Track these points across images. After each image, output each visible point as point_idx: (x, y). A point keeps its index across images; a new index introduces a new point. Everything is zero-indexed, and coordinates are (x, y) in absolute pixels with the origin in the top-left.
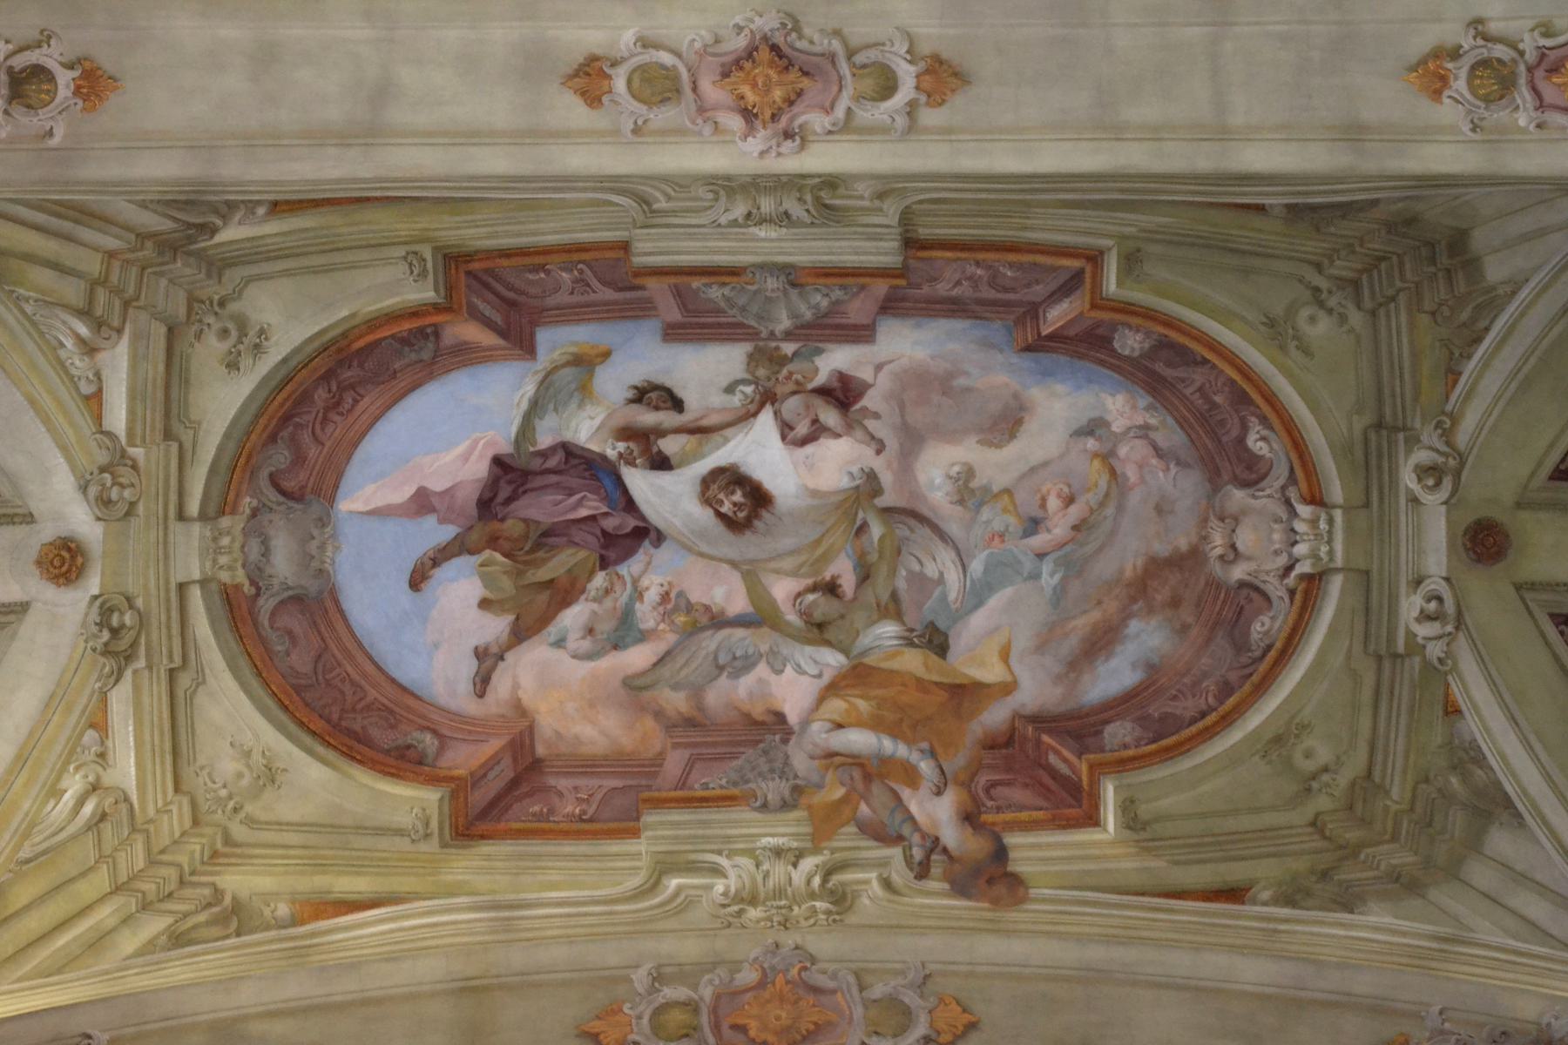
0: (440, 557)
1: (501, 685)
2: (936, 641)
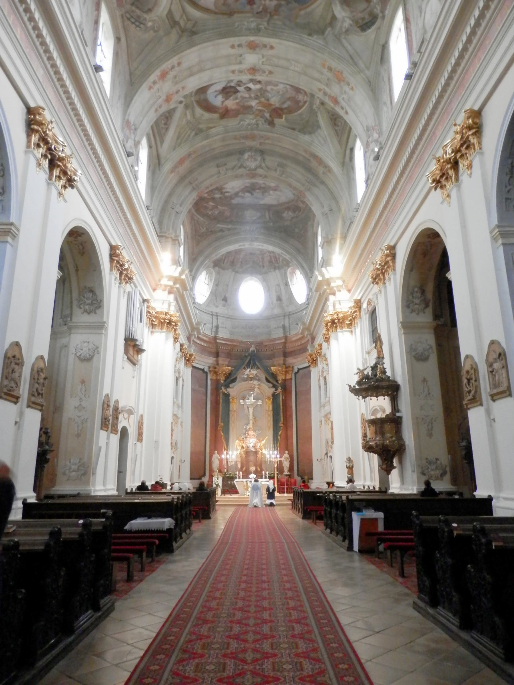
0: (217, 95)
1: (224, 104)
2: (268, 100)
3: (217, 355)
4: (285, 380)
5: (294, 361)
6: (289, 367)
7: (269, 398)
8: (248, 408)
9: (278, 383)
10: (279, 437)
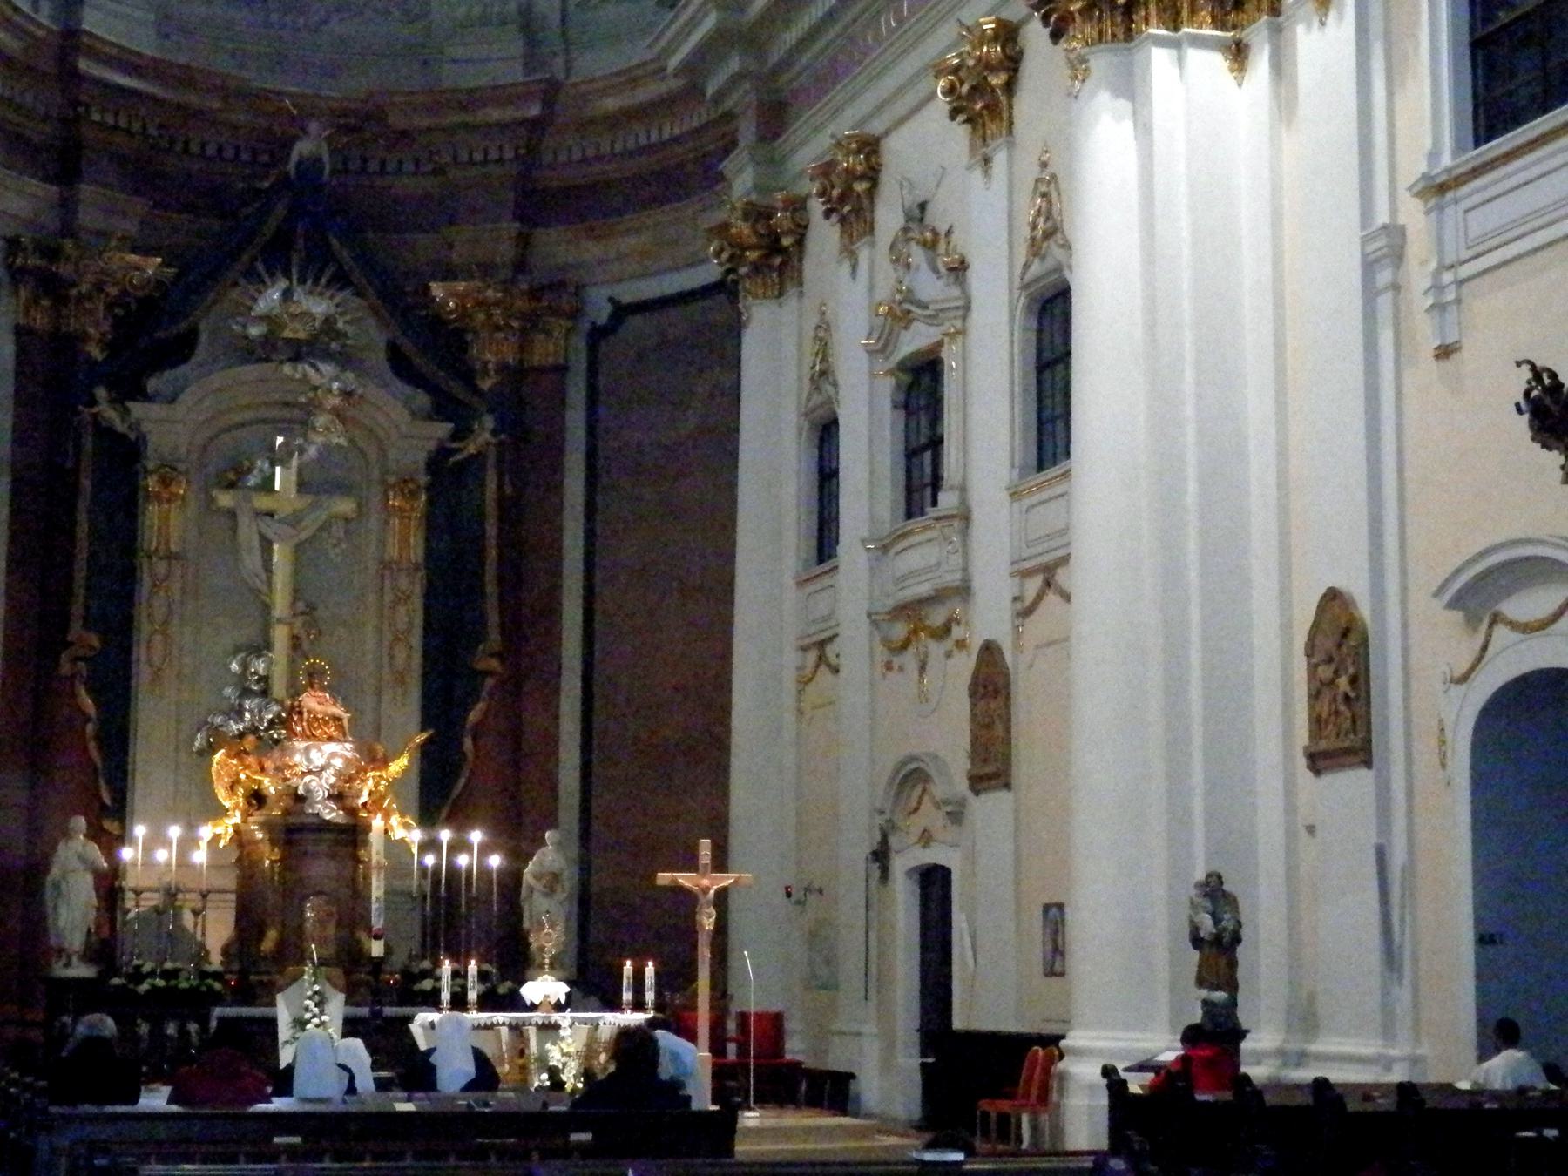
4: (516, 374)
5: (592, 250)
6: (559, 286)
7: (405, 485)
8: (266, 545)
9: (476, 391)
10: (468, 743)
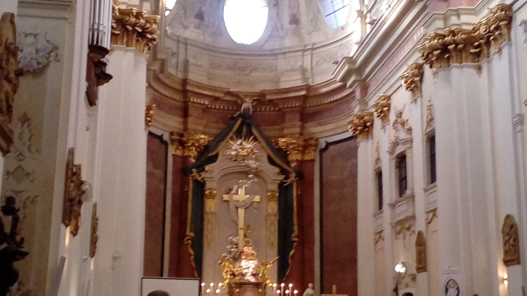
3: (185, 113)
4: (301, 162)
5: (320, 129)
6: (311, 138)
8: (237, 208)
9: (290, 166)
